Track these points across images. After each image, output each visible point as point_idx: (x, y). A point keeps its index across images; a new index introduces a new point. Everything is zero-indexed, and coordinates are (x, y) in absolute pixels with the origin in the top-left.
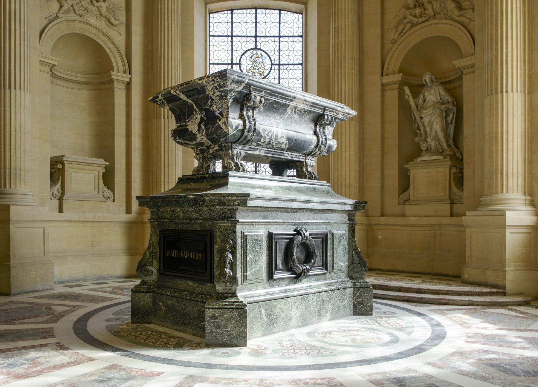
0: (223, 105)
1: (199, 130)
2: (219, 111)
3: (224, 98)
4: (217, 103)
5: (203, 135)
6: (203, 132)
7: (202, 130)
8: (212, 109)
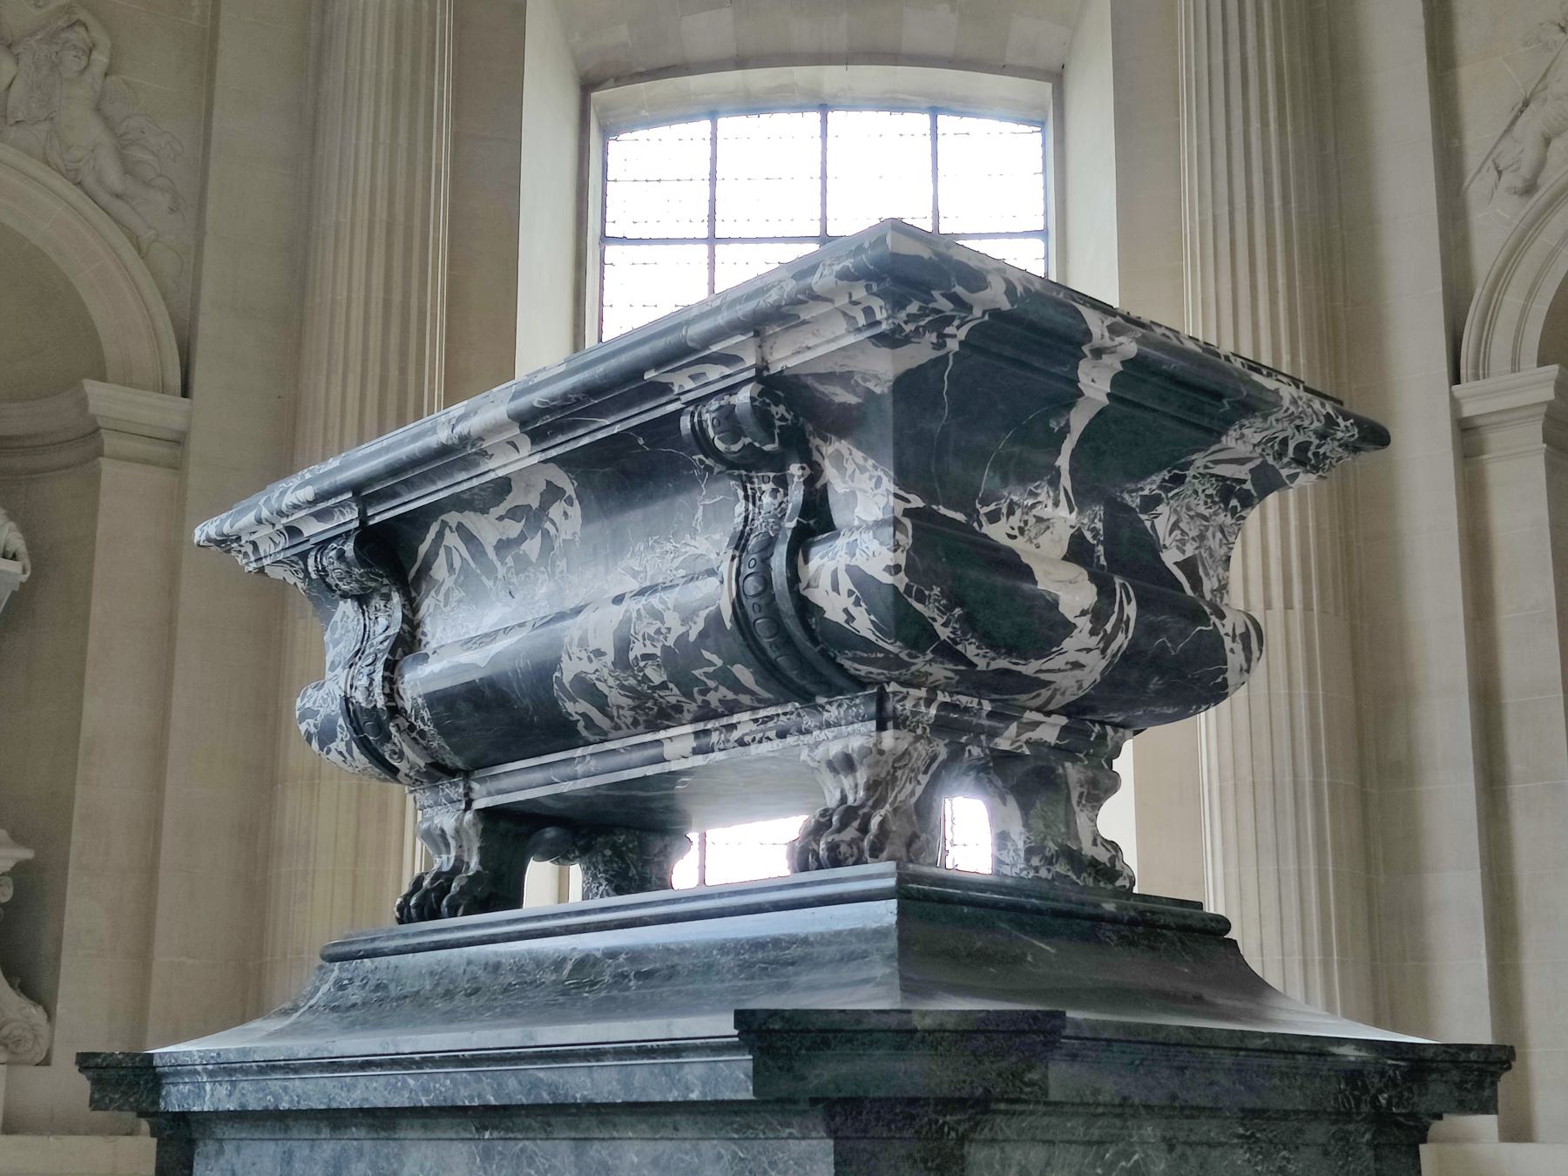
0: (1209, 534)
1: (1098, 615)
2: (1183, 552)
3: (1234, 502)
4: (1189, 508)
5: (1103, 651)
6: (1121, 638)
7: (1119, 620)
8: (1148, 524)
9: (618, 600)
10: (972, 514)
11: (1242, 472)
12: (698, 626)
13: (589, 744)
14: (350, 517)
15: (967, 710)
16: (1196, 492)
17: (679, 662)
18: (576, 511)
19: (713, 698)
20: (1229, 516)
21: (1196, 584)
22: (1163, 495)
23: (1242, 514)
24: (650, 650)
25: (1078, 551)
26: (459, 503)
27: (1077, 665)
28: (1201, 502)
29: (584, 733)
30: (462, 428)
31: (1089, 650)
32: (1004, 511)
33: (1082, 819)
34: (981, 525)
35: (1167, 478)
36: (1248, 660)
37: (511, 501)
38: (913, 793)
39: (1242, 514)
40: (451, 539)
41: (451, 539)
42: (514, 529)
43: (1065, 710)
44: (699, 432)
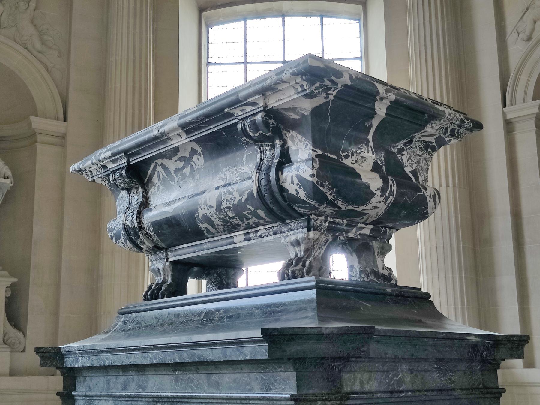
0: (421, 161)
1: (383, 190)
3: (430, 150)
4: (414, 152)
5: (385, 202)
7: (391, 191)
8: (400, 158)
9: (217, 188)
10: (339, 156)
11: (432, 139)
12: (246, 196)
13: (208, 238)
14: (124, 161)
15: (338, 224)
16: (416, 147)
17: (239, 209)
18: (202, 158)
19: (251, 222)
20: (428, 155)
21: (417, 178)
22: (405, 148)
23: (433, 154)
24: (229, 205)
25: (376, 168)
26: (161, 156)
27: (376, 207)
28: (418, 150)
29: (207, 234)
30: (162, 130)
31: (380, 202)
32: (350, 154)
33: (379, 260)
34: (342, 160)
35: (406, 142)
36: (435, 204)
37: (179, 155)
38: (320, 253)
39: (433, 154)
40: (159, 168)
41: (159, 168)
42: (180, 164)
43: (372, 223)
44: (244, 130)
